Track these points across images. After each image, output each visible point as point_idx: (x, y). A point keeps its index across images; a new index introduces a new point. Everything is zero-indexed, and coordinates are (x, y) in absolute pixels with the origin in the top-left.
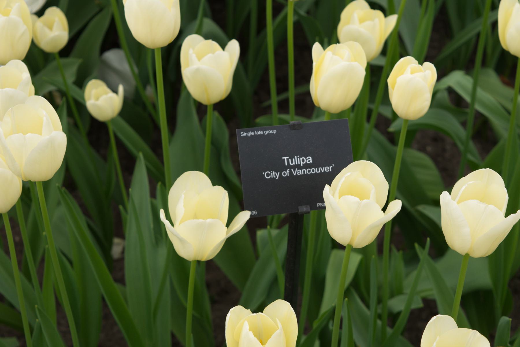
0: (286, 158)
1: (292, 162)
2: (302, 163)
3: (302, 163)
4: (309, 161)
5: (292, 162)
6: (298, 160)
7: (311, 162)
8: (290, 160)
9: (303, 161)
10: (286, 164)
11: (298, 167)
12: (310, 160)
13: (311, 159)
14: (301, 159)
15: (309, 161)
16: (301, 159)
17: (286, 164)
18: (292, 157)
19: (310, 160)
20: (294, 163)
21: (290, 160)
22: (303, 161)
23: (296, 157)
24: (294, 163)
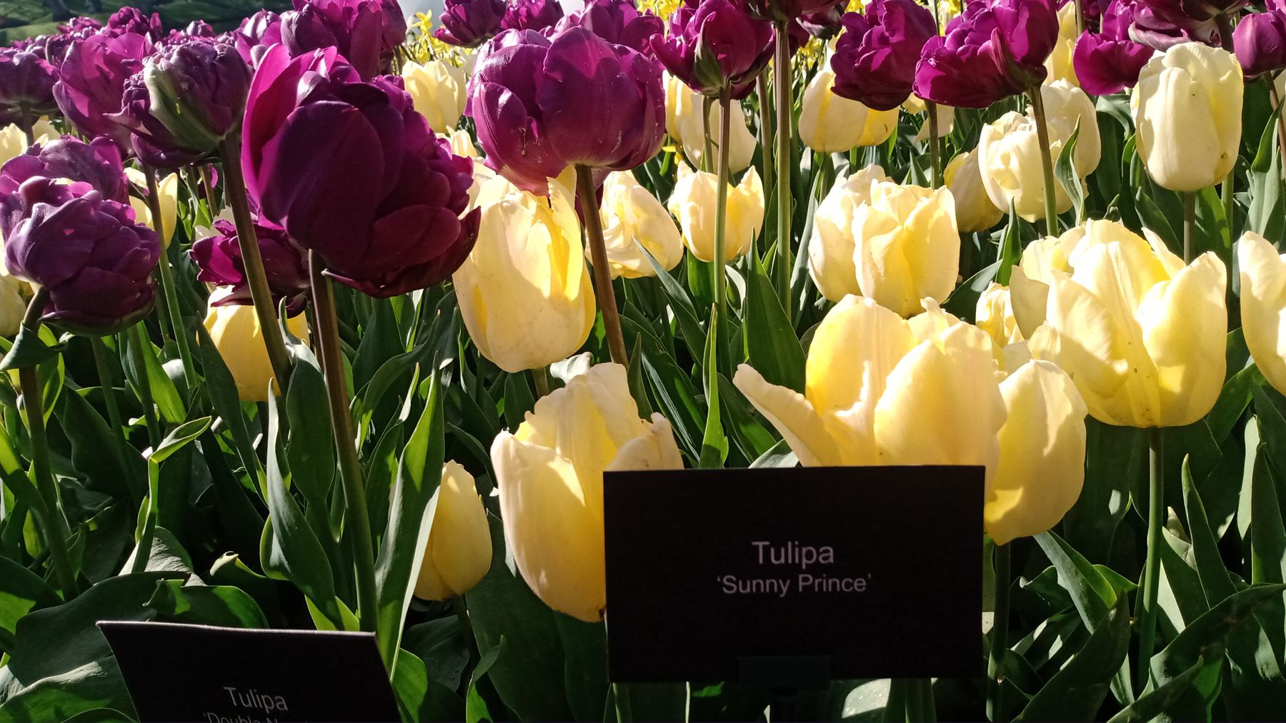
0: (761, 544)
1: (778, 558)
3: (804, 561)
4: (824, 559)
5: (778, 558)
7: (831, 560)
8: (772, 550)
9: (809, 555)
10: (761, 561)
11: (790, 572)
12: (829, 555)
13: (831, 554)
14: (804, 550)
17: (761, 561)
18: (778, 544)
21: (772, 550)
22: (809, 555)
23: (790, 544)
24: (783, 560)
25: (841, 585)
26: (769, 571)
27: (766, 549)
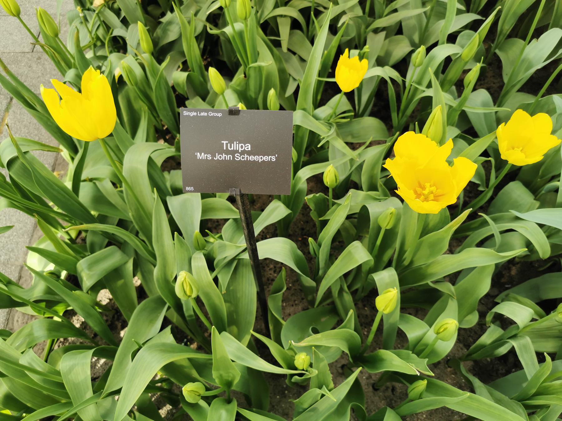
0: (225, 142)
1: (231, 147)
2: (240, 149)
3: (240, 149)
4: (248, 148)
5: (231, 147)
6: (236, 146)
7: (250, 149)
12: (248, 147)
13: (250, 147)
14: (240, 145)
15: (248, 148)
16: (240, 145)
18: (231, 142)
19: (248, 147)
20: (232, 149)
25: (252, 158)
26: (227, 152)
27: (227, 144)
